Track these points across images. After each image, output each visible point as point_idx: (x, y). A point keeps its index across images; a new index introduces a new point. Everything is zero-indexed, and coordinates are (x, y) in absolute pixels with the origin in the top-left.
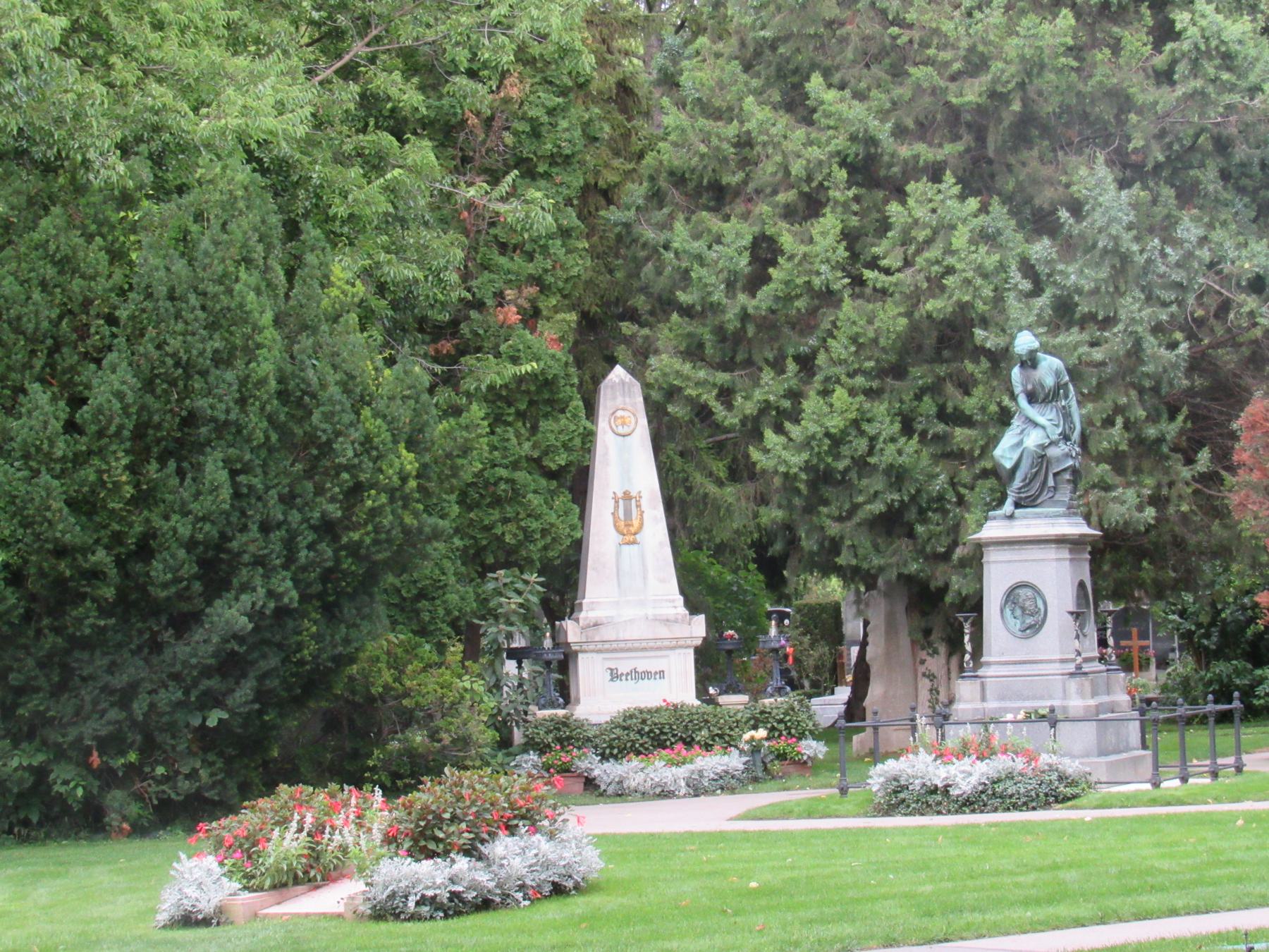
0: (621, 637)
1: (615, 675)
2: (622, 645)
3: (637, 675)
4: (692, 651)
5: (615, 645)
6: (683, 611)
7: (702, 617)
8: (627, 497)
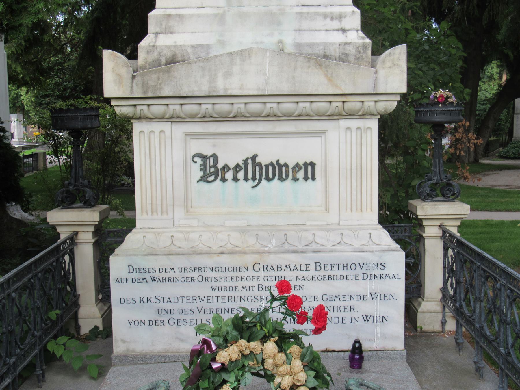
0: (221, 85)
1: (211, 170)
2: (223, 106)
4: (374, 125)
5: (206, 107)
6: (357, 37)
7: (400, 52)
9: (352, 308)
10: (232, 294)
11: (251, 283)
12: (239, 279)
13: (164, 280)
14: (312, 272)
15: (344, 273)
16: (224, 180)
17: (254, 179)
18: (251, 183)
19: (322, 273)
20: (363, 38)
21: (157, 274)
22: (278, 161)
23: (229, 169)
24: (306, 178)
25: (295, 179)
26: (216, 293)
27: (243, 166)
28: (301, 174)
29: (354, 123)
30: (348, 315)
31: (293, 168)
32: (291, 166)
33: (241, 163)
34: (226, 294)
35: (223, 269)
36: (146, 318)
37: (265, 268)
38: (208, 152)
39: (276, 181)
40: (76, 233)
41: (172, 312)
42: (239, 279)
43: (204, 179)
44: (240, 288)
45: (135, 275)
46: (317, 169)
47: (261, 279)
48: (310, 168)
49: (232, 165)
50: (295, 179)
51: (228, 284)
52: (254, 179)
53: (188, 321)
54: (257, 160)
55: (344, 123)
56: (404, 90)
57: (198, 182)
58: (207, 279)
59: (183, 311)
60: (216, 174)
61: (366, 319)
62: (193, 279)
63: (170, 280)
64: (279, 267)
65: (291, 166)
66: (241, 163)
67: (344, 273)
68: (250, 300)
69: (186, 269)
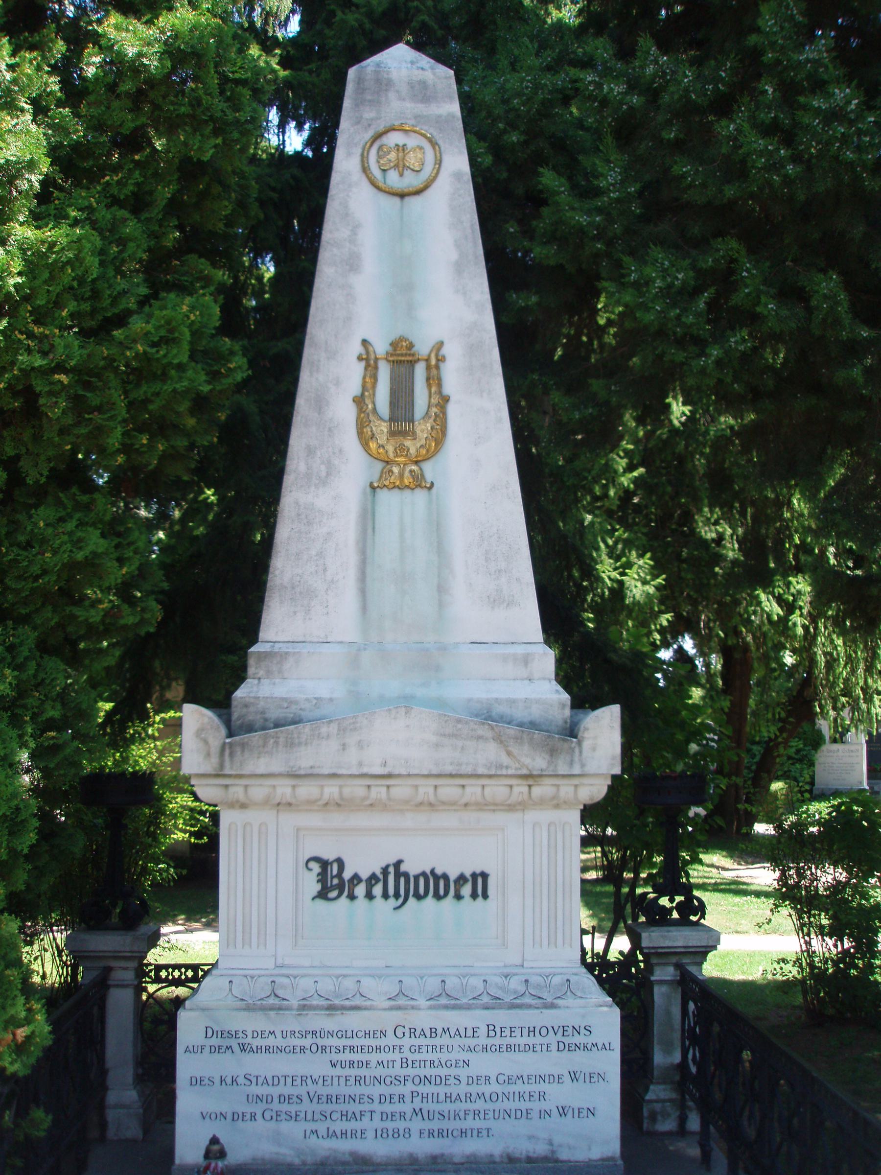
1: (333, 881)
3: (402, 884)
5: (331, 790)
8: (403, 357)
9: (542, 1096)
10: (362, 1072)
11: (390, 1056)
12: (372, 1049)
13: (259, 1049)
14: (483, 1040)
15: (531, 1041)
16: (352, 897)
17: (397, 895)
18: (392, 902)
19: (497, 1041)
20: (557, 691)
21: (249, 1040)
22: (432, 871)
23: (360, 880)
24: (474, 896)
25: (458, 897)
26: (338, 1071)
27: (381, 877)
28: (466, 890)
29: (546, 816)
30: (536, 1106)
31: (457, 881)
32: (453, 877)
33: (378, 873)
34: (353, 1072)
35: (349, 1034)
36: (226, 1108)
37: (413, 1032)
38: (329, 856)
39: (430, 900)
40: (108, 970)
41: (269, 1099)
42: (372, 1049)
43: (322, 895)
44: (373, 1064)
45: (215, 1041)
46: (491, 882)
47: (406, 1049)
48: (480, 881)
49: (365, 875)
50: (458, 897)
51: (355, 1057)
52: (397, 895)
53: (293, 1115)
54: (403, 868)
55: (531, 816)
56: (617, 770)
57: (313, 899)
58: (324, 1049)
59: (285, 1099)
60: (341, 887)
61: (563, 1111)
62: (303, 1049)
63: (268, 1049)
64: (433, 1031)
65: (453, 877)
66: (378, 873)
67: (531, 1041)
68: (388, 1082)
69: (293, 1033)
